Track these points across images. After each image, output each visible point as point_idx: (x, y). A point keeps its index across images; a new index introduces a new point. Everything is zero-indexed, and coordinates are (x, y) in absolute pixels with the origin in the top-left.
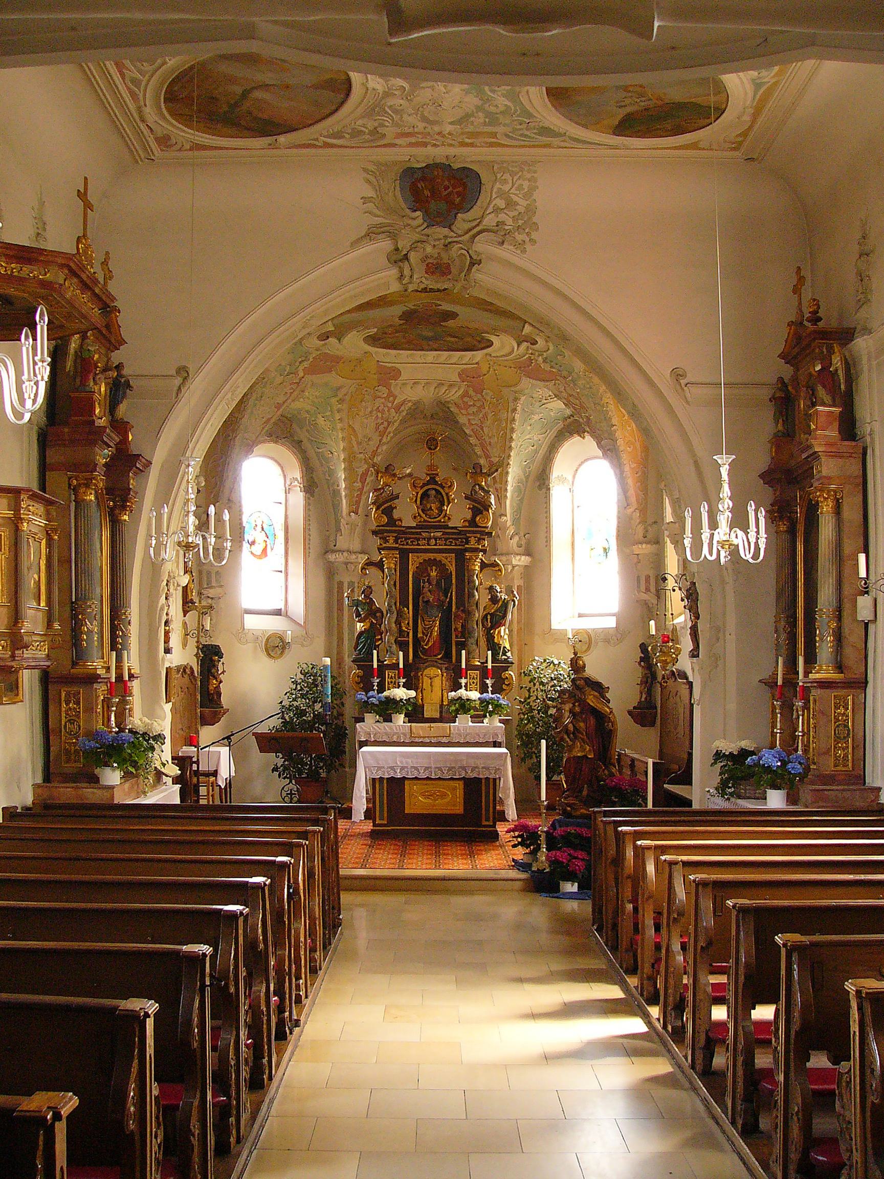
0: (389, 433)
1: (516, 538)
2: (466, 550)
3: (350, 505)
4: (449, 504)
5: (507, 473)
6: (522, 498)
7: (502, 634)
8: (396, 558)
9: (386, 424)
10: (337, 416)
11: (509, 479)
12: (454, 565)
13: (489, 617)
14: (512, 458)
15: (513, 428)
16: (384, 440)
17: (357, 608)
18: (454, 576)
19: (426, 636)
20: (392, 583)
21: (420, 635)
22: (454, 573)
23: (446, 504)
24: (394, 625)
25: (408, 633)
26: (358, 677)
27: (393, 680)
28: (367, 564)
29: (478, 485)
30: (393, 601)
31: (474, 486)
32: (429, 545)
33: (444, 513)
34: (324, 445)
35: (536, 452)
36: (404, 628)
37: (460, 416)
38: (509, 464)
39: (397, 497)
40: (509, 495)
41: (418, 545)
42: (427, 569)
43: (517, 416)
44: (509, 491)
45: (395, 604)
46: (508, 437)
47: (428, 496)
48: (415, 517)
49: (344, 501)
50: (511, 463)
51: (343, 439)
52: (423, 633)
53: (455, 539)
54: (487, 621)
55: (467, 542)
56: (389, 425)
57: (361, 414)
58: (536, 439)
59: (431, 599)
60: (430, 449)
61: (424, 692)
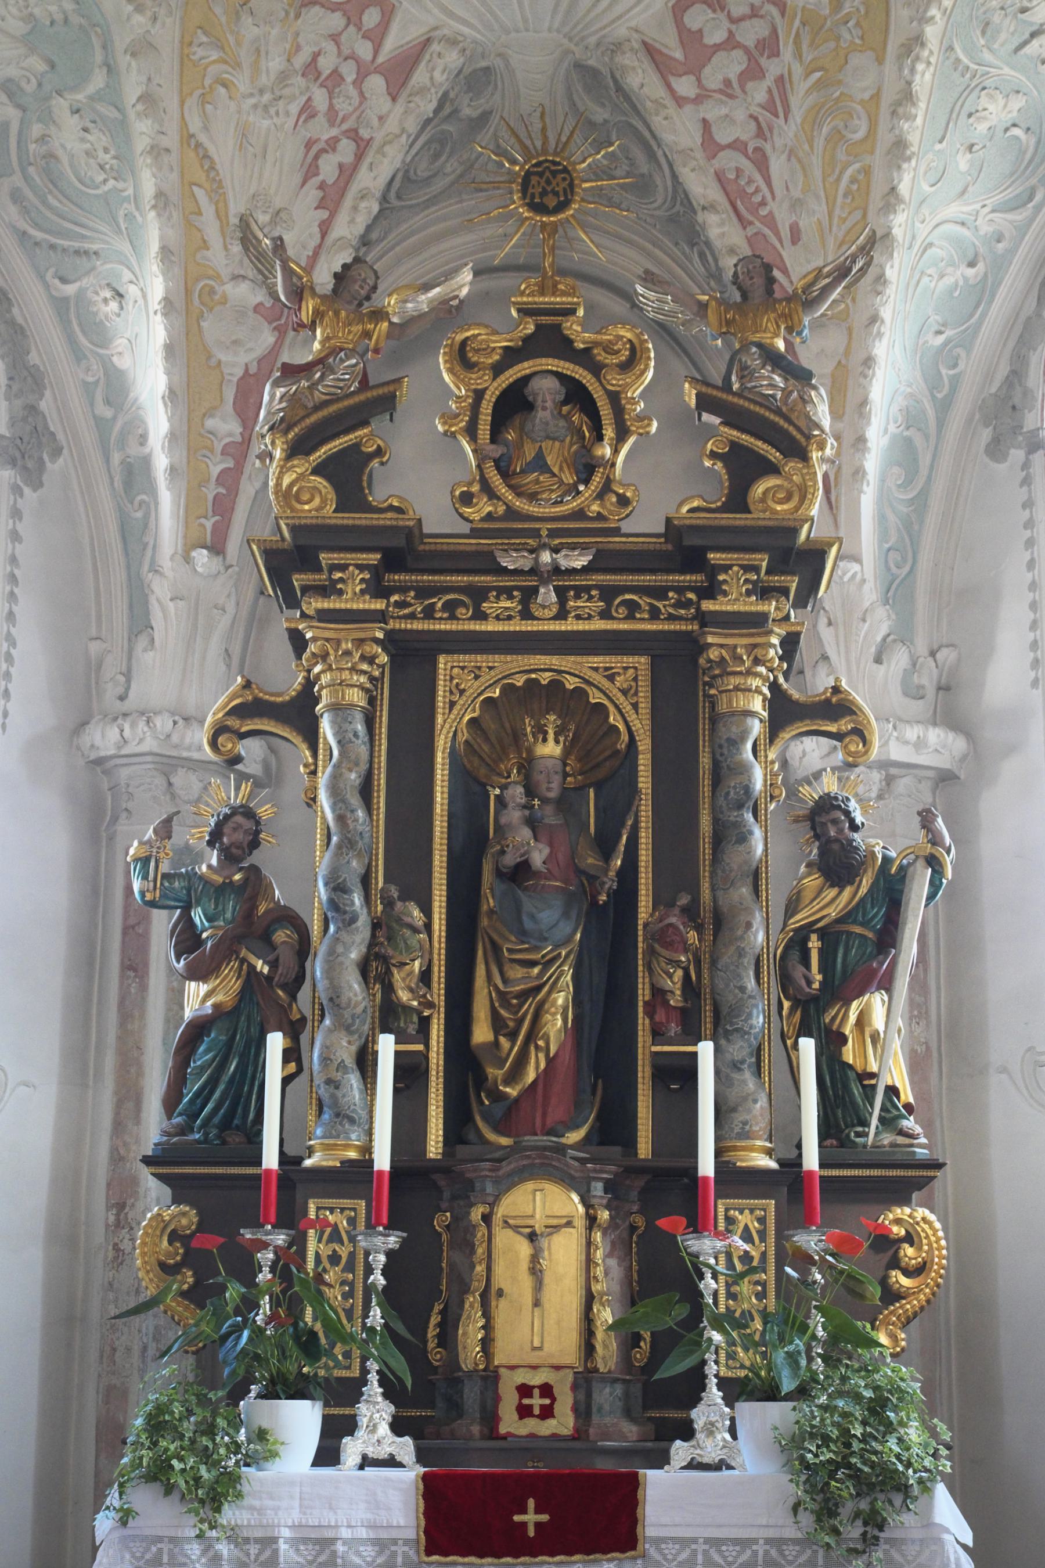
1: (899, 659)
3: (189, 513)
5: (869, 361)
6: (923, 496)
8: (371, 660)
9: (346, 151)
12: (645, 706)
13: (814, 943)
14: (890, 291)
17: (186, 919)
19: (513, 1036)
21: (481, 1033)
22: (644, 744)
23: (609, 432)
24: (354, 987)
25: (425, 1023)
26: (173, 1237)
27: (344, 1252)
28: (240, 711)
31: (745, 347)
32: (526, 614)
33: (597, 479)
36: (404, 996)
37: (672, 109)
38: (874, 319)
41: (480, 616)
42: (517, 737)
43: (923, 79)
45: (366, 881)
46: (878, 191)
47: (529, 407)
49: (166, 499)
50: (886, 313)
52: (497, 1023)
53: (660, 593)
54: (806, 962)
56: (359, 157)
57: (242, 83)
58: (985, 229)
59: (538, 857)
61: (502, 1311)
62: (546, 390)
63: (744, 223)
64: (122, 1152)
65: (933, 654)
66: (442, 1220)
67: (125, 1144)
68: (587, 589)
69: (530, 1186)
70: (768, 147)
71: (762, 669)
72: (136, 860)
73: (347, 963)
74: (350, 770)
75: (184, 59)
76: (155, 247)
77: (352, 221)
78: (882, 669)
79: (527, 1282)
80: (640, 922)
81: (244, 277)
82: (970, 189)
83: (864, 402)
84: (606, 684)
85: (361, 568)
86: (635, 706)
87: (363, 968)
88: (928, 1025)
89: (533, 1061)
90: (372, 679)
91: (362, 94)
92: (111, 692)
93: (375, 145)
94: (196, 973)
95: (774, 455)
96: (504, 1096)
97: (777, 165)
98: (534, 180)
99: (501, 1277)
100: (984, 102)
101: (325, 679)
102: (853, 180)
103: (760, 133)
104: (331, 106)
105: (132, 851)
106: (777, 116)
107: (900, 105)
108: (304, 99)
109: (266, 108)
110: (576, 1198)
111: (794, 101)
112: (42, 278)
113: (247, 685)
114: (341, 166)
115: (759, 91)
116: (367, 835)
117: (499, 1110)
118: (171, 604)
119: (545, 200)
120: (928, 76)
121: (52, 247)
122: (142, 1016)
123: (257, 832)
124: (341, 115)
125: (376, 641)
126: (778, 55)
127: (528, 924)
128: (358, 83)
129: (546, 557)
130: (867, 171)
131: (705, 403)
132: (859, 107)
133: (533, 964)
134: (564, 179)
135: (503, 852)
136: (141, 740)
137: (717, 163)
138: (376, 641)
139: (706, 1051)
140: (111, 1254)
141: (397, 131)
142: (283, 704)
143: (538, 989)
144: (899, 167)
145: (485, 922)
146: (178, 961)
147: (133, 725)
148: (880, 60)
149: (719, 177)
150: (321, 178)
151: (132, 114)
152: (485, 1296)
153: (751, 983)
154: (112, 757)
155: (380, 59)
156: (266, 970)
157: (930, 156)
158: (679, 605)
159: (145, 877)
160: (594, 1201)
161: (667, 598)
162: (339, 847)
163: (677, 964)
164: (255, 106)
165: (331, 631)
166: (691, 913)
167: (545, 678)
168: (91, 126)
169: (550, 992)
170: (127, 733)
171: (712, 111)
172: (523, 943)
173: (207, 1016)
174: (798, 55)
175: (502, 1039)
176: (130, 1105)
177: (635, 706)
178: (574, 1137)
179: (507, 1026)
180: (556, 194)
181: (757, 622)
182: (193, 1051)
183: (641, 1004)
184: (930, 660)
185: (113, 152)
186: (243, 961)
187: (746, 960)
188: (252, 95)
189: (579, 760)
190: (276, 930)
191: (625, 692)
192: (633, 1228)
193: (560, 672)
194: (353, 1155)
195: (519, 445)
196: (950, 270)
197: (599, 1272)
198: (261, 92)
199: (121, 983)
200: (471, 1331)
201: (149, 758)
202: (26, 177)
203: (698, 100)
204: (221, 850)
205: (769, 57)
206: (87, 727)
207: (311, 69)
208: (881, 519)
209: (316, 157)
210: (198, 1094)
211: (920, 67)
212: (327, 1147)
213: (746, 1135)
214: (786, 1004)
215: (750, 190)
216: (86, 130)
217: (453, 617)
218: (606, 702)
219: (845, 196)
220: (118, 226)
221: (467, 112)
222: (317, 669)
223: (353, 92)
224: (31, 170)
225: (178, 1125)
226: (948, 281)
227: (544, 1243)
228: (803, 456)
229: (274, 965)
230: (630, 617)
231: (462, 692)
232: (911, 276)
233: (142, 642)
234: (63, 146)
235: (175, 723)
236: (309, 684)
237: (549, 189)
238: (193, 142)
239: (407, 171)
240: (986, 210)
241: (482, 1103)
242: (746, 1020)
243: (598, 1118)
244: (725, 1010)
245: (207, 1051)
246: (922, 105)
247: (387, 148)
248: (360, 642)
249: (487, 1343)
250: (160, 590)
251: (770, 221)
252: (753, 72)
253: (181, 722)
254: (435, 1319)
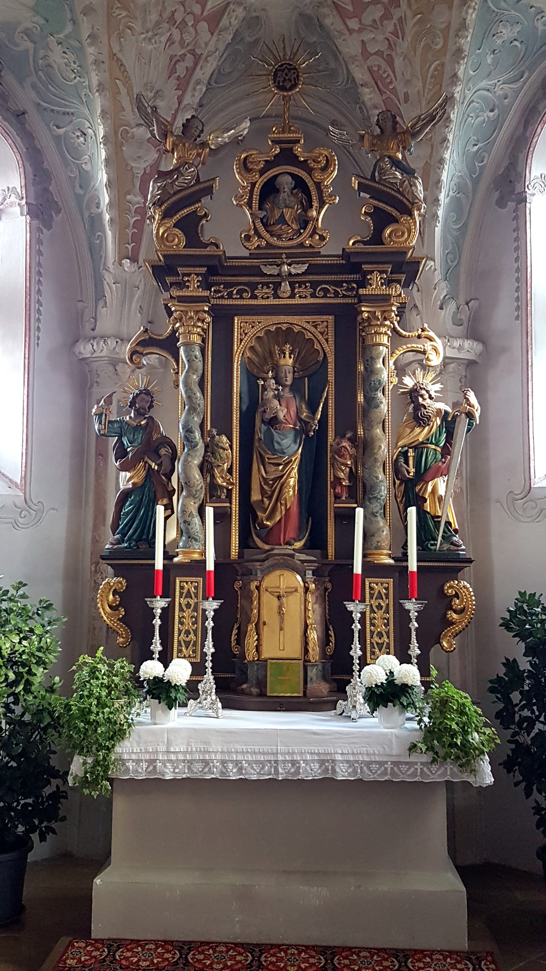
0: (198, 83)
1: (451, 307)
2: (361, 299)
3: (121, 241)
4: (321, 207)
5: (442, 161)
6: (465, 225)
7: (441, 491)
9: (189, 61)
10: (85, 32)
11: (444, 177)
12: (331, 339)
15: (460, 50)
16: (187, 100)
17: (120, 441)
18: (331, 367)
19: (270, 498)
20: (195, 378)
21: (256, 496)
22: (331, 359)
23: (315, 204)
24: (196, 475)
25: (230, 492)
26: (115, 593)
27: (192, 602)
28: (143, 343)
29: (389, 157)
30: (197, 420)
31: (382, 159)
32: (276, 296)
33: (310, 226)
34: (67, 118)
35: (496, 125)
36: (220, 481)
39: (209, 191)
40: (440, 213)
42: (271, 354)
44: (442, 202)
45: (202, 426)
46: (446, 76)
48: (248, 238)
49: (109, 233)
50: (450, 138)
51: (101, 87)
52: (263, 492)
53: (339, 284)
54: (407, 463)
55: (363, 283)
57: (137, 26)
59: (281, 415)
60: (282, 88)
61: (265, 631)
62: (286, 182)
63: (381, 92)
65: (467, 304)
66: (238, 585)
68: (304, 283)
69: (278, 572)
70: (393, 54)
71: (387, 323)
72: (96, 415)
73: (193, 466)
74: (194, 374)
75: (109, 15)
76: (99, 111)
77: (193, 96)
78: (443, 312)
79: (277, 618)
80: (329, 443)
81: (142, 125)
82: (493, 72)
83: (439, 181)
84: (313, 329)
85: (197, 275)
86: (327, 340)
87: (201, 468)
88: (462, 479)
89: (279, 510)
90: (203, 329)
91: (196, 31)
92: (88, 326)
93: (204, 57)
94: (123, 468)
95: (395, 213)
96: (267, 526)
97: (398, 62)
98: (279, 73)
99: (265, 617)
100: (501, 29)
101: (181, 330)
102: (436, 69)
103: (390, 46)
104: (182, 38)
105: (94, 411)
106: (398, 38)
107: (460, 31)
108: (169, 34)
109: (150, 39)
110: (299, 578)
111: (407, 31)
112: (48, 126)
113: (146, 331)
114: (187, 68)
115: (390, 27)
116: (202, 405)
117: (264, 533)
118: (114, 286)
119: (285, 84)
120: (474, 16)
121: (52, 111)
123: (152, 402)
124: (187, 42)
125: (205, 312)
126: (400, 6)
127: (276, 446)
128: (194, 26)
129: (286, 268)
130: (442, 65)
131: (362, 187)
132: (439, 32)
133: (280, 465)
134: (294, 73)
135: (265, 411)
136: (102, 350)
137: (369, 63)
138: (205, 312)
139: (360, 512)
141: (214, 50)
142: (163, 340)
143: (282, 477)
144: (458, 63)
145: (257, 444)
147: (98, 344)
148: (450, 8)
149: (370, 69)
150: (177, 74)
151: (85, 44)
152: (257, 625)
153: (381, 476)
154: (88, 358)
155: (205, 14)
156: (156, 468)
157: (474, 56)
158: (347, 290)
159: (100, 423)
160: (307, 580)
161: (342, 286)
162: (189, 410)
163: (346, 465)
164: (144, 39)
165: (182, 307)
166: (353, 440)
167: (284, 327)
168: (66, 50)
169: (287, 478)
170: (95, 347)
171: (367, 36)
172: (274, 455)
173: (129, 488)
174: (409, 5)
175: (265, 499)
177: (327, 340)
178: (298, 545)
179: (267, 493)
180: (290, 80)
181: (385, 299)
182: (124, 504)
183: (329, 482)
184: (466, 306)
185: (78, 63)
186: (146, 462)
187: (378, 464)
188: (143, 33)
189: (300, 364)
190: (160, 448)
191: (322, 333)
192: (326, 589)
193: (292, 324)
194: (196, 556)
195: (272, 210)
196: (481, 114)
197: (310, 614)
198: (147, 32)
200: (251, 641)
201: (106, 359)
202: (39, 78)
203: (360, 31)
204: (135, 410)
205: (395, 8)
206: (78, 344)
207: (172, 20)
208: (444, 238)
209: (176, 63)
210: (126, 525)
211: (470, 11)
212: (184, 553)
213: (378, 548)
214: (398, 482)
215: (385, 76)
216: (64, 52)
217: (241, 298)
218: (313, 338)
219: (432, 78)
220: (82, 100)
221: (248, 39)
222: (178, 325)
223: (192, 30)
224: (40, 73)
225: (117, 539)
226: (480, 119)
227: (284, 600)
228: (411, 215)
229: (159, 465)
230: (325, 296)
231: (246, 334)
232: (463, 118)
234: (55, 61)
235: (117, 342)
236: (174, 331)
237: (287, 78)
238: (115, 58)
239: (219, 70)
240: (500, 83)
241: (256, 528)
242: (378, 493)
243: (309, 535)
244: (368, 488)
245: (130, 505)
246: (471, 31)
247: (208, 58)
248: (197, 312)
249: (258, 648)
250: (108, 279)
251: (394, 91)
252: (387, 16)
253: (120, 342)
254: (235, 632)
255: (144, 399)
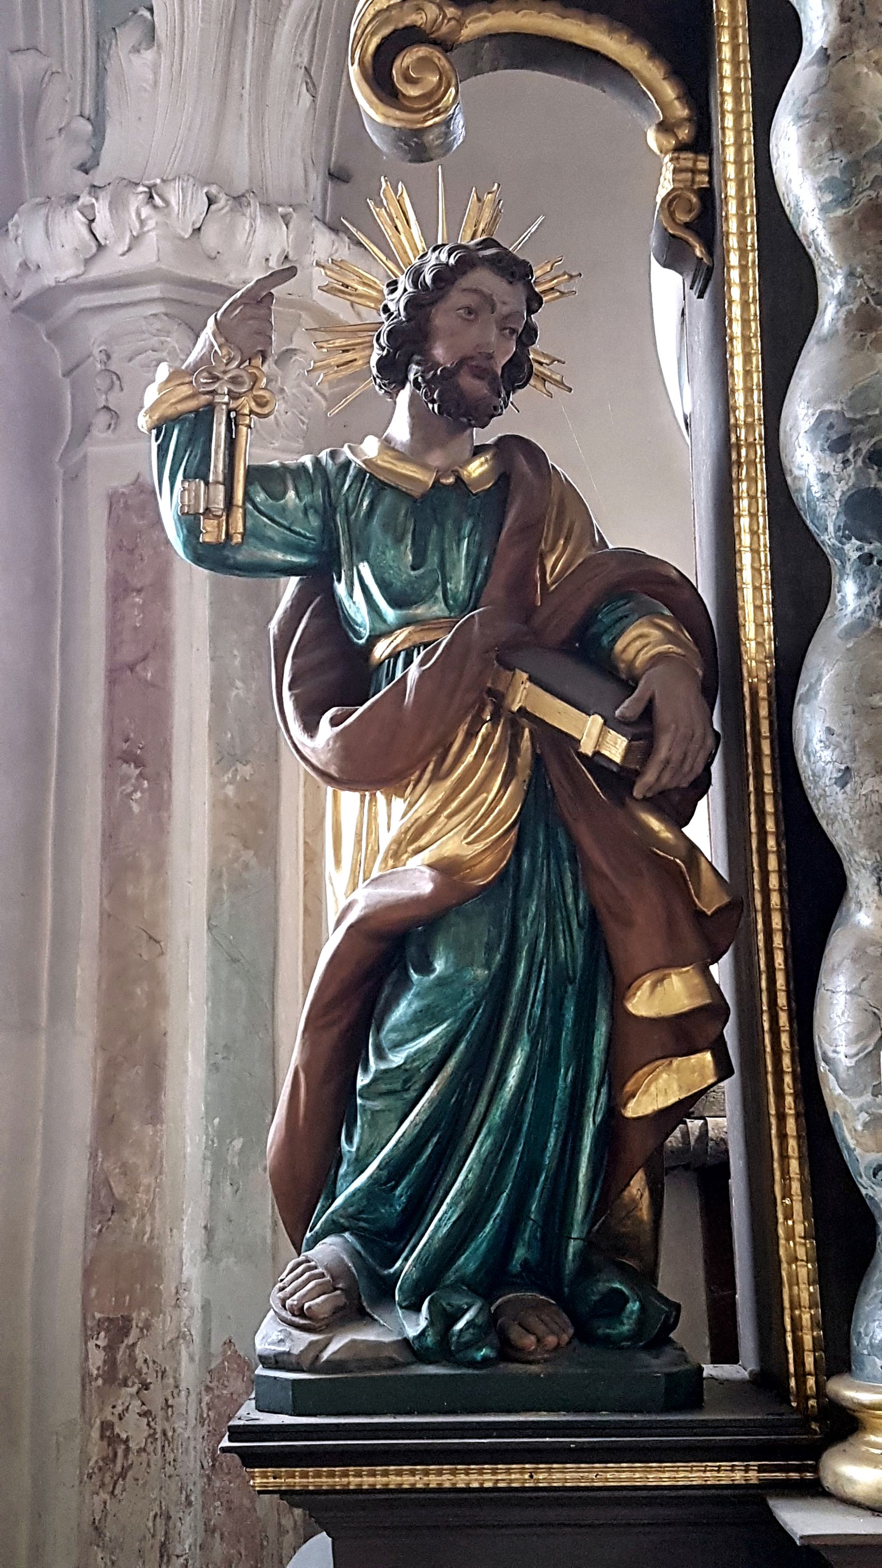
64: (118, 1190)
67: (126, 1170)
122: (160, 866)
136: (136, 240)
140: (96, 1449)
146: (311, 728)
147: (116, 206)
170: (102, 225)
173: (417, 901)
176: (136, 1074)
199: (108, 793)
233: (128, 36)
235: (211, 202)
253: (222, 200)
255: (489, 302)
